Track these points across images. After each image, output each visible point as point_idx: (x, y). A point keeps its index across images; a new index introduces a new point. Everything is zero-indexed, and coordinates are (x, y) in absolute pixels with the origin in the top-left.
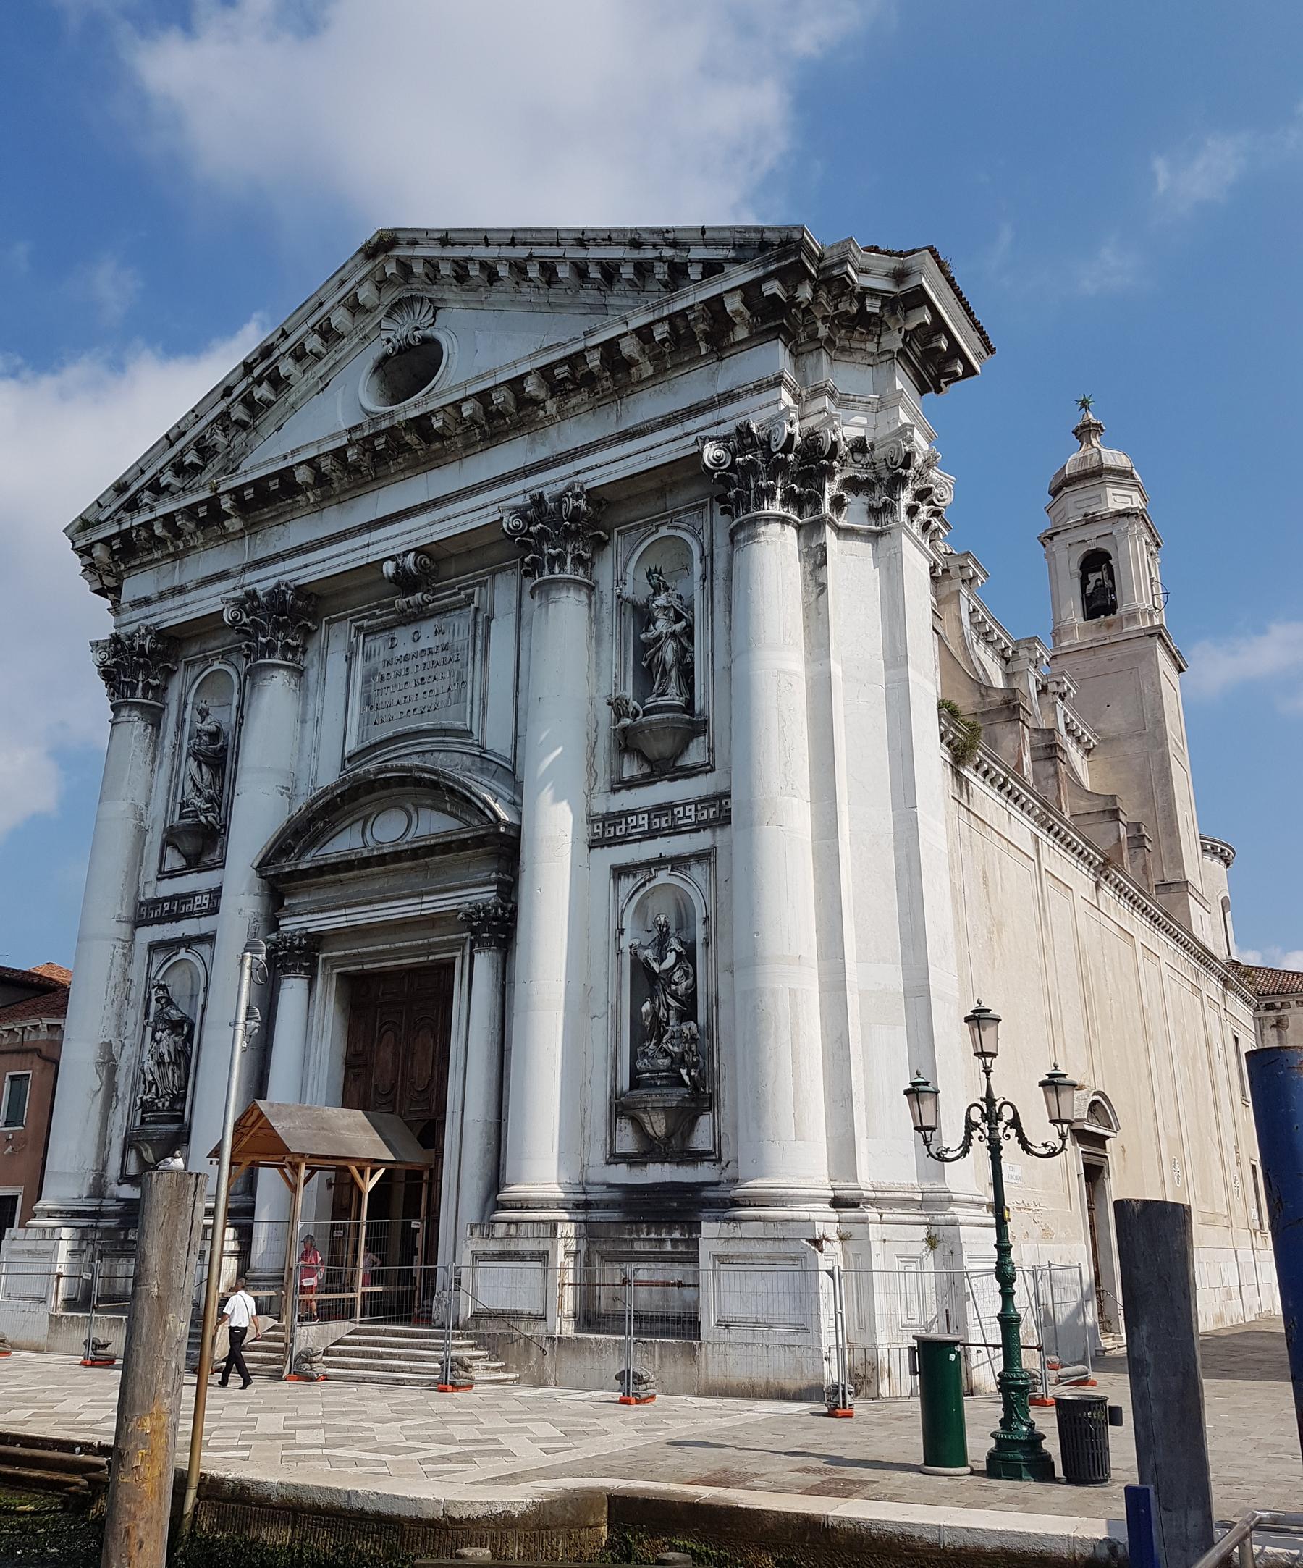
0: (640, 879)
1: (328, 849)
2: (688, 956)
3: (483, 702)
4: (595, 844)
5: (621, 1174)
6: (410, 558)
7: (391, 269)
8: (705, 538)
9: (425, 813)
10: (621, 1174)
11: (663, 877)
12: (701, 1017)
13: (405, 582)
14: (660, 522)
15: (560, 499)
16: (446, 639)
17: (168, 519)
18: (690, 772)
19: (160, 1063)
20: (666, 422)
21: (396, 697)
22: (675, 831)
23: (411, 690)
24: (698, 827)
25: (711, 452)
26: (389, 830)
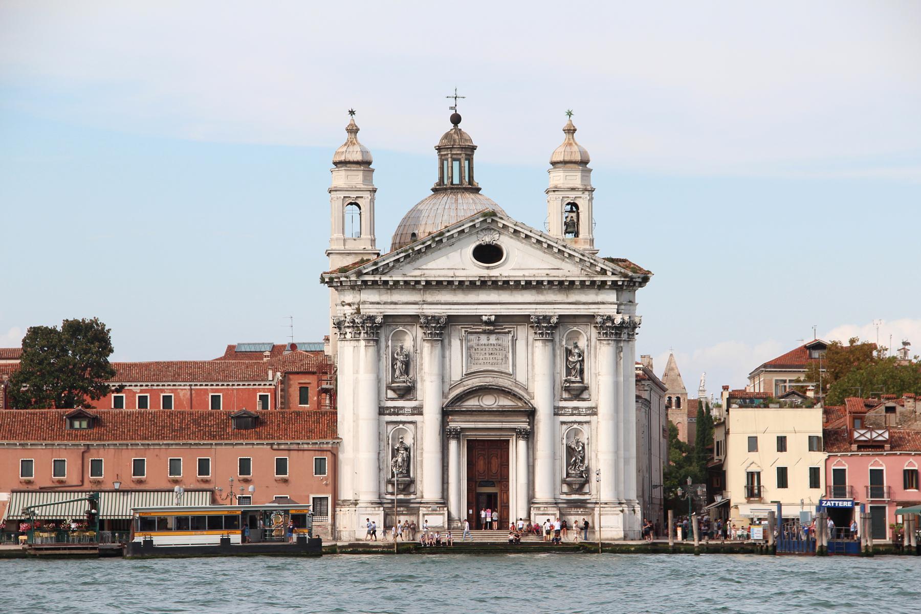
0: (569, 425)
1: (466, 404)
2: (583, 448)
3: (514, 365)
4: (555, 414)
5: (564, 497)
6: (493, 318)
7: (489, 220)
8: (589, 334)
9: (501, 398)
10: (564, 497)
11: (575, 426)
12: (586, 462)
13: (488, 323)
14: (575, 326)
15: (551, 317)
16: (500, 342)
17: (396, 283)
18: (584, 400)
19: (403, 460)
20: (584, 304)
21: (481, 357)
22: (580, 415)
23: (487, 356)
24: (586, 415)
25: (599, 320)
26: (488, 402)
